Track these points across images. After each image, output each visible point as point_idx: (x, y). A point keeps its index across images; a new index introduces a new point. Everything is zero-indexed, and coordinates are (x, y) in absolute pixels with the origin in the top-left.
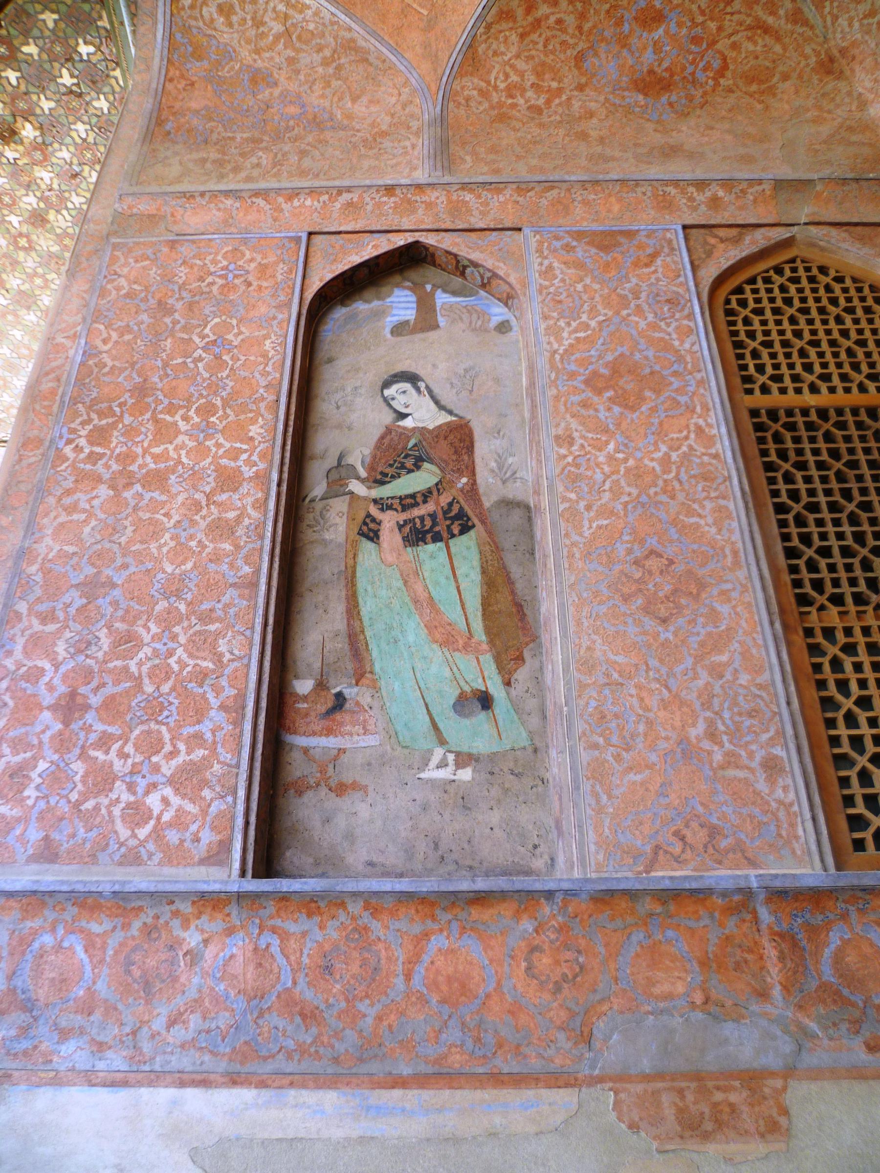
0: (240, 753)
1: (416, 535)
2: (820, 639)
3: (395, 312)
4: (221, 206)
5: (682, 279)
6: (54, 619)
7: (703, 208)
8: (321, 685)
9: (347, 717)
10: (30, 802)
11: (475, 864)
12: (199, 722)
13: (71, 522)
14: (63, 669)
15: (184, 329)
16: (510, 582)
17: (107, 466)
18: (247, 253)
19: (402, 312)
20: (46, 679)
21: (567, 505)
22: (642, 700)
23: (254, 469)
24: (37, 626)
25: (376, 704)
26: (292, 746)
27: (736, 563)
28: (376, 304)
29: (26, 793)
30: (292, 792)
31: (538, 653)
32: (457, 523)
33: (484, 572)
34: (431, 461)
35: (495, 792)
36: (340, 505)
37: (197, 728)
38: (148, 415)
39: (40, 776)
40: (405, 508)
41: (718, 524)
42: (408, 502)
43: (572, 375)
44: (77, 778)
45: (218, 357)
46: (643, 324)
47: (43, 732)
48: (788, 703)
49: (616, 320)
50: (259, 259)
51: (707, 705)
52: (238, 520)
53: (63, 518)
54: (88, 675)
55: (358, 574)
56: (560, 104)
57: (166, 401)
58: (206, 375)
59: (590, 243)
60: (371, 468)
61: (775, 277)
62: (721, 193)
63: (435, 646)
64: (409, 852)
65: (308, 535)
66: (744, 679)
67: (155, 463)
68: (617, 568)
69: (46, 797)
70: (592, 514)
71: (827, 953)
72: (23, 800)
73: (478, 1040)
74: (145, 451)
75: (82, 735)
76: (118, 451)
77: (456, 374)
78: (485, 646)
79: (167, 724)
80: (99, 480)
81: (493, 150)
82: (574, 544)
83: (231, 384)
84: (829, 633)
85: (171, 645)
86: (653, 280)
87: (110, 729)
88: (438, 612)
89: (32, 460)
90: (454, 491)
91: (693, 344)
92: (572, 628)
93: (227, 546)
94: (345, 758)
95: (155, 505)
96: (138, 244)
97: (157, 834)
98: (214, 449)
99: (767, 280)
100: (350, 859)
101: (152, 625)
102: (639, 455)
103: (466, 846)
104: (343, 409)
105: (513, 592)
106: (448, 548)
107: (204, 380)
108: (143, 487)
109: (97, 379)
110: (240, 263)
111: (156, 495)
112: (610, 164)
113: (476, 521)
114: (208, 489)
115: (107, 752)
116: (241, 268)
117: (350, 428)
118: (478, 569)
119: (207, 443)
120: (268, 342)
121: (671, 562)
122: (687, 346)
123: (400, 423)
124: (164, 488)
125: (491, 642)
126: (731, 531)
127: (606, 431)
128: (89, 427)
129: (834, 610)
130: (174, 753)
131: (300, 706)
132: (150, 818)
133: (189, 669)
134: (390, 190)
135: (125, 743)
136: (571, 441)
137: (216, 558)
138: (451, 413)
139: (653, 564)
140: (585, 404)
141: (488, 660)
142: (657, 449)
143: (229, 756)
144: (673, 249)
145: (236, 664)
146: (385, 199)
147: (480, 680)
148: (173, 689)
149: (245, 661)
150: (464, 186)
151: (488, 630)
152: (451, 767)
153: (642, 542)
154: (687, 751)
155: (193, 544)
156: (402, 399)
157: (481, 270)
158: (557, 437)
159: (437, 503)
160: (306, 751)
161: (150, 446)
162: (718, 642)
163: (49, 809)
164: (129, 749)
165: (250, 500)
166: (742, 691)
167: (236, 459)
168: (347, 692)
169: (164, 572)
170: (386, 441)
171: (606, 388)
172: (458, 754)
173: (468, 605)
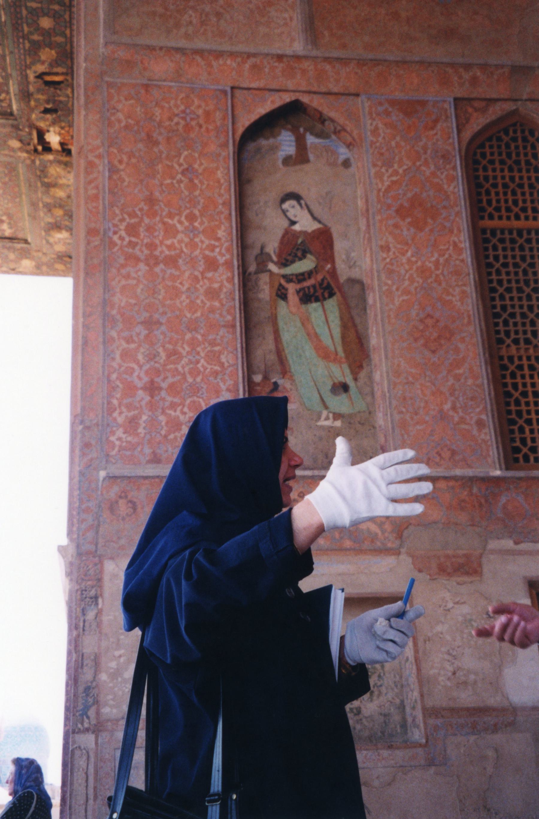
1: (307, 298)
5: (451, 141)
6: (133, 342)
8: (266, 378)
13: (128, 285)
15: (168, 158)
16: (355, 326)
19: (288, 149)
20: (136, 374)
21: (387, 287)
22: (422, 391)
23: (224, 258)
24: (124, 345)
27: (469, 323)
28: (271, 141)
31: (369, 364)
33: (342, 319)
34: (311, 253)
36: (264, 278)
39: (144, 422)
40: (299, 281)
41: (462, 300)
42: (301, 277)
43: (389, 207)
45: (191, 180)
46: (428, 173)
47: (141, 401)
50: (203, 107)
51: (452, 394)
52: (221, 288)
53: (123, 282)
54: (158, 372)
58: (187, 193)
60: (279, 256)
61: (504, 137)
64: (315, 460)
71: (500, 504)
74: (161, 243)
78: (344, 360)
79: (202, 398)
82: (391, 310)
83: (202, 201)
84: (511, 359)
85: (198, 357)
86: (434, 140)
88: (320, 341)
89: (97, 243)
91: (455, 188)
92: (390, 355)
93: (217, 304)
95: (173, 278)
96: (123, 84)
98: (200, 244)
101: (185, 346)
102: (423, 259)
105: (357, 331)
106: (323, 306)
113: (336, 290)
115: (175, 411)
118: (338, 319)
120: (219, 172)
121: (438, 321)
122: (451, 188)
124: (177, 267)
125: (347, 357)
127: (407, 244)
128: (124, 224)
133: (208, 370)
134: (280, 58)
135: (184, 406)
137: (212, 310)
138: (320, 222)
139: (429, 322)
140: (396, 226)
141: (345, 367)
144: (447, 117)
146: (276, 64)
148: (202, 380)
149: (235, 367)
150: (326, 59)
151: (345, 351)
153: (424, 309)
154: (443, 416)
157: (336, 124)
158: (381, 247)
159: (316, 279)
162: (457, 364)
164: (186, 409)
165: (224, 277)
167: (213, 251)
168: (280, 382)
169: (186, 317)
172: (334, 414)
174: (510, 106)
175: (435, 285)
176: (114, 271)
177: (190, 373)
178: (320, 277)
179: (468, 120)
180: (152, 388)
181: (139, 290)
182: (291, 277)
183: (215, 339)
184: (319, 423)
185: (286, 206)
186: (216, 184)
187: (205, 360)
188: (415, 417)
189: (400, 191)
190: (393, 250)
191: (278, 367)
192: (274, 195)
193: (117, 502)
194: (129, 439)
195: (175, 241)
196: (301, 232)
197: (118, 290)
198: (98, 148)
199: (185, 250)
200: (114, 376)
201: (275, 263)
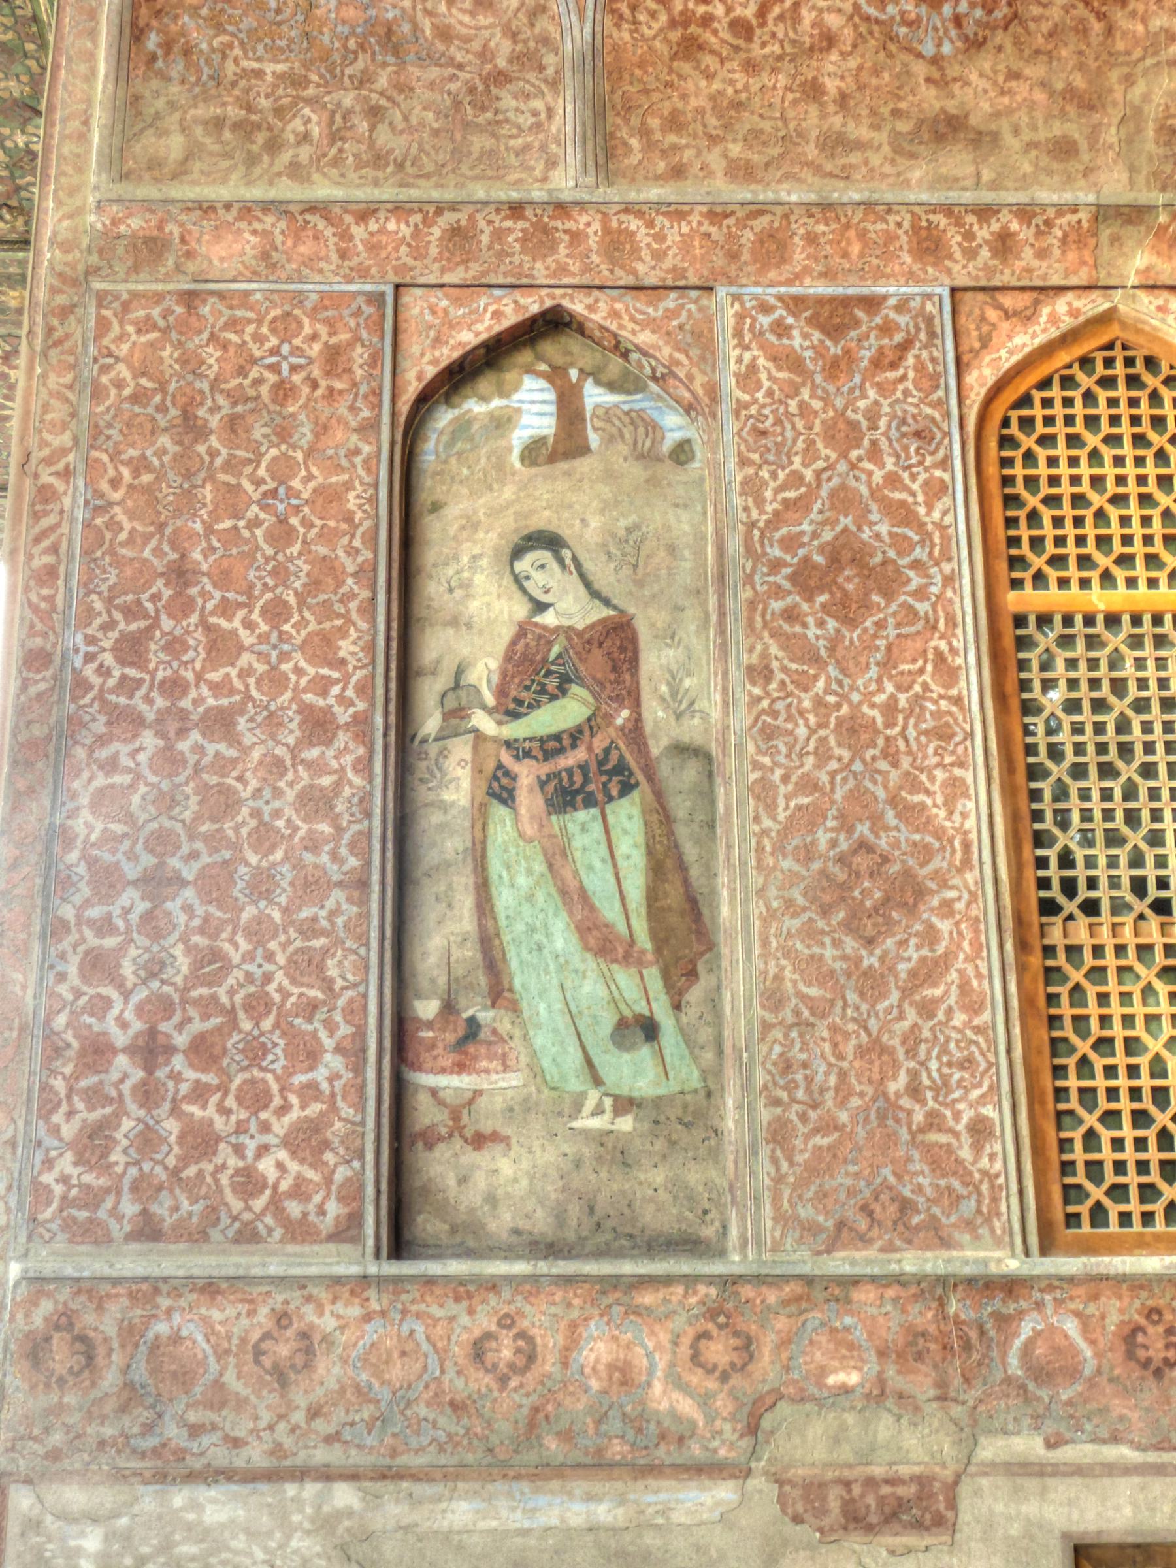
1: (565, 796)
2: (1061, 960)
4: (257, 226)
5: (941, 393)
7: (985, 253)
8: (449, 1008)
9: (483, 1050)
10: (119, 1169)
12: (311, 1069)
14: (135, 999)
16: (682, 868)
17: (148, 700)
20: (115, 1012)
22: (835, 1045)
24: (92, 940)
25: (517, 1033)
26: (418, 1087)
28: (496, 403)
29: (113, 1158)
30: (420, 1145)
31: (714, 968)
33: (650, 852)
34: (582, 683)
35: (660, 1145)
36: (461, 749)
38: (194, 619)
40: (548, 755)
42: (550, 746)
43: (776, 566)
44: (173, 1139)
46: (878, 476)
48: (1009, 1051)
52: (338, 786)
53: (101, 781)
54: (166, 1007)
55: (491, 853)
56: (781, 18)
57: (218, 595)
58: (270, 552)
60: (501, 692)
61: (1081, 377)
62: (1014, 226)
64: (560, 1218)
65: (422, 793)
66: (959, 1019)
68: (816, 865)
69: (137, 1163)
71: (1018, 1343)
72: (110, 1166)
73: (640, 1430)
74: (199, 677)
75: (171, 1084)
76: (160, 675)
77: (613, 535)
78: (650, 957)
80: (138, 722)
81: (674, 122)
82: (765, 832)
84: (1073, 951)
85: (268, 967)
87: (204, 1078)
88: (592, 908)
89: (42, 686)
90: (612, 732)
91: (945, 513)
94: (483, 1102)
95: (222, 765)
96: (135, 295)
97: (276, 1204)
99: (1068, 382)
100: (492, 1226)
101: (240, 939)
104: (458, 593)
105: (686, 882)
107: (267, 560)
109: (112, 552)
110: (297, 342)
111: (222, 747)
112: (855, 158)
113: (640, 777)
114: (291, 740)
115: (204, 1107)
116: (297, 351)
117: (469, 626)
120: (351, 496)
121: (885, 859)
122: (936, 515)
124: (233, 739)
125: (658, 950)
126: (964, 815)
127: (816, 660)
128: (114, 635)
129: (1083, 921)
130: (285, 1109)
132: (265, 1186)
134: (516, 209)
135: (226, 1093)
136: (768, 676)
137: (313, 844)
138: (607, 602)
139: (862, 862)
142: (881, 690)
144: (932, 335)
145: (350, 993)
146: (509, 224)
148: (277, 1025)
151: (654, 935)
152: (608, 1115)
153: (850, 830)
155: (280, 823)
156: (539, 578)
158: (750, 669)
159: (590, 749)
160: (434, 1092)
163: (142, 1176)
164: (230, 1102)
165: (348, 759)
166: (954, 1035)
167: (324, 693)
170: (520, 647)
171: (821, 589)
172: (616, 1098)
174: (1092, 305)
175: (883, 765)
176: (80, 753)
177: (248, 1007)
178: (599, 744)
179: (985, 341)
180: (151, 1050)
181: (136, 799)
183: (315, 919)
184: (577, 1124)
185: (523, 565)
188: (813, 1115)
189: (806, 527)
192: (491, 539)
193: (48, 1339)
194: (88, 1178)
195: (233, 673)
196: (557, 630)
197: (85, 801)
198: (64, 452)
199: (254, 693)
200: (61, 1020)
201: (489, 711)
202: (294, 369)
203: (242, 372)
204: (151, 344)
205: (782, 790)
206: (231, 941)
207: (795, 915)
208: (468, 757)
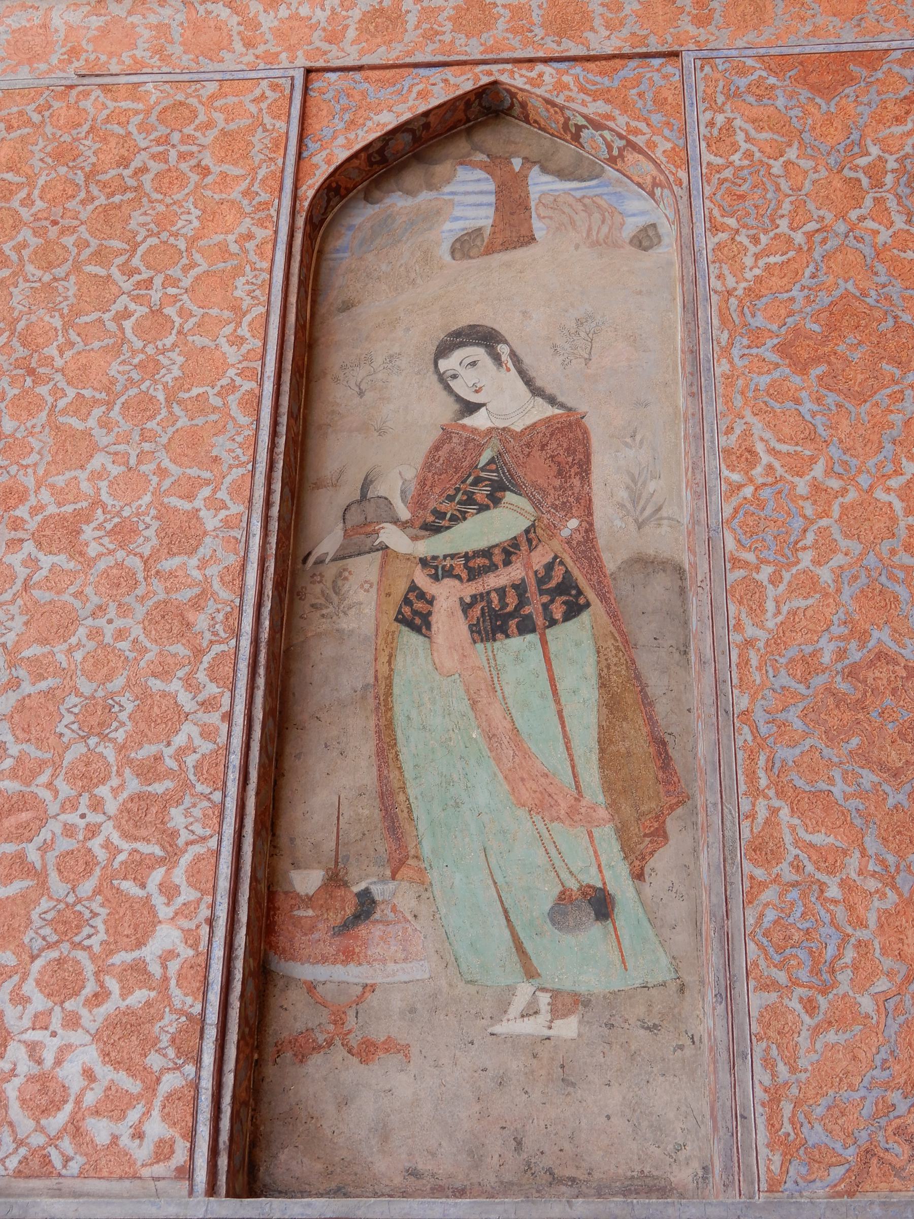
0: (205, 994)
1: (494, 621)
3: (457, 212)
8: (336, 879)
9: (377, 931)
11: (580, 1175)
16: (647, 703)
18: (201, 109)
19: (470, 212)
21: (740, 573)
22: (851, 908)
26: (289, 980)
28: (425, 196)
32: (560, 599)
33: (603, 684)
36: (365, 569)
37: (136, 954)
40: (474, 574)
42: (478, 563)
46: (884, 236)
49: (841, 227)
55: (396, 690)
57: (71, 393)
58: (139, 344)
59: (803, 79)
60: (418, 503)
63: (522, 813)
64: (476, 1157)
67: (59, 505)
70: (782, 587)
78: (603, 813)
82: (749, 643)
88: (527, 754)
90: (556, 545)
93: (181, 650)
94: (373, 1000)
98: (155, 480)
100: (381, 1165)
101: (62, 785)
103: (567, 1146)
104: (369, 396)
105: (651, 720)
106: (544, 643)
108: (39, 545)
110: (189, 130)
111: (61, 559)
113: (591, 595)
116: (187, 139)
117: (381, 432)
118: (594, 681)
119: (143, 468)
123: (468, 421)
124: (76, 550)
125: (613, 805)
127: (812, 437)
130: (100, 997)
131: (301, 913)
133: (122, 857)
135: (23, 979)
138: (552, 400)
139: (881, 675)
141: (606, 835)
143: (189, 1000)
147: (594, 870)
148: (97, 891)
149: (213, 843)
151: (608, 786)
152: (544, 1016)
153: (863, 637)
155: (124, 645)
158: (728, 452)
159: (527, 566)
160: (311, 987)
161: (47, 473)
168: (377, 891)
169: (79, 694)
172: (556, 994)
173: (575, 743)
178: (540, 558)
182: (448, 563)
183: (158, 758)
186: (227, 314)
187: (118, 827)
190: (765, 458)
191: (382, 846)
199: (105, 497)
202: (182, 156)
203: (124, 162)
204: (23, 139)
205: (771, 591)
206: (50, 785)
207: (793, 744)
208: (374, 577)
